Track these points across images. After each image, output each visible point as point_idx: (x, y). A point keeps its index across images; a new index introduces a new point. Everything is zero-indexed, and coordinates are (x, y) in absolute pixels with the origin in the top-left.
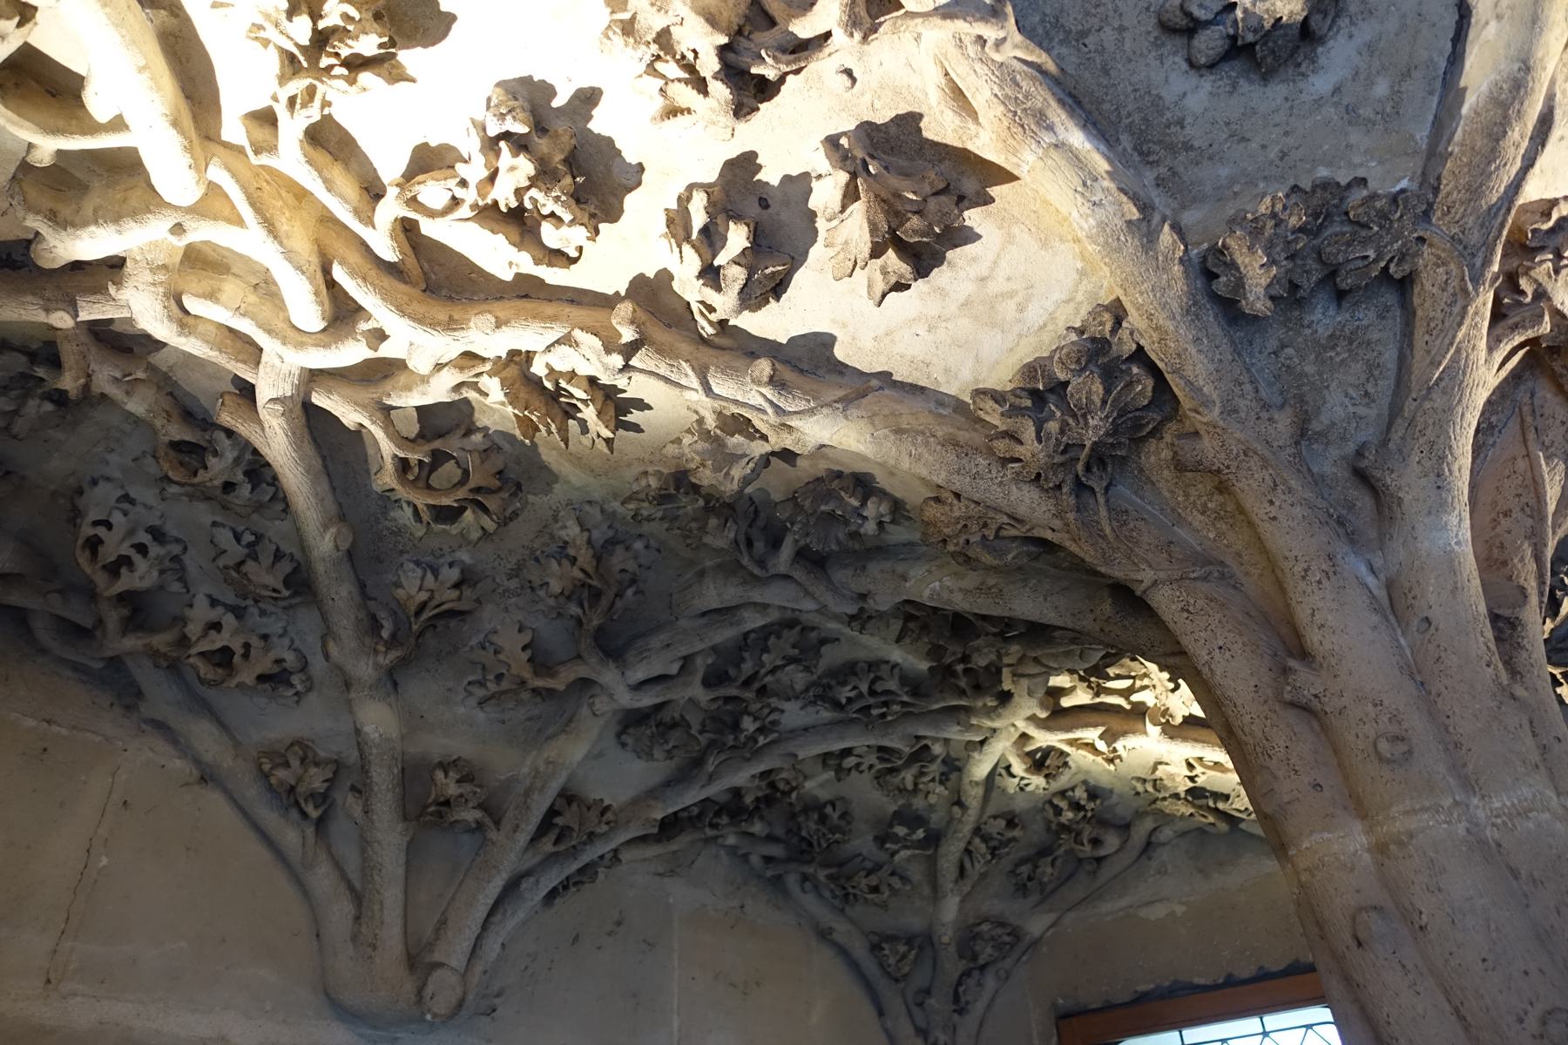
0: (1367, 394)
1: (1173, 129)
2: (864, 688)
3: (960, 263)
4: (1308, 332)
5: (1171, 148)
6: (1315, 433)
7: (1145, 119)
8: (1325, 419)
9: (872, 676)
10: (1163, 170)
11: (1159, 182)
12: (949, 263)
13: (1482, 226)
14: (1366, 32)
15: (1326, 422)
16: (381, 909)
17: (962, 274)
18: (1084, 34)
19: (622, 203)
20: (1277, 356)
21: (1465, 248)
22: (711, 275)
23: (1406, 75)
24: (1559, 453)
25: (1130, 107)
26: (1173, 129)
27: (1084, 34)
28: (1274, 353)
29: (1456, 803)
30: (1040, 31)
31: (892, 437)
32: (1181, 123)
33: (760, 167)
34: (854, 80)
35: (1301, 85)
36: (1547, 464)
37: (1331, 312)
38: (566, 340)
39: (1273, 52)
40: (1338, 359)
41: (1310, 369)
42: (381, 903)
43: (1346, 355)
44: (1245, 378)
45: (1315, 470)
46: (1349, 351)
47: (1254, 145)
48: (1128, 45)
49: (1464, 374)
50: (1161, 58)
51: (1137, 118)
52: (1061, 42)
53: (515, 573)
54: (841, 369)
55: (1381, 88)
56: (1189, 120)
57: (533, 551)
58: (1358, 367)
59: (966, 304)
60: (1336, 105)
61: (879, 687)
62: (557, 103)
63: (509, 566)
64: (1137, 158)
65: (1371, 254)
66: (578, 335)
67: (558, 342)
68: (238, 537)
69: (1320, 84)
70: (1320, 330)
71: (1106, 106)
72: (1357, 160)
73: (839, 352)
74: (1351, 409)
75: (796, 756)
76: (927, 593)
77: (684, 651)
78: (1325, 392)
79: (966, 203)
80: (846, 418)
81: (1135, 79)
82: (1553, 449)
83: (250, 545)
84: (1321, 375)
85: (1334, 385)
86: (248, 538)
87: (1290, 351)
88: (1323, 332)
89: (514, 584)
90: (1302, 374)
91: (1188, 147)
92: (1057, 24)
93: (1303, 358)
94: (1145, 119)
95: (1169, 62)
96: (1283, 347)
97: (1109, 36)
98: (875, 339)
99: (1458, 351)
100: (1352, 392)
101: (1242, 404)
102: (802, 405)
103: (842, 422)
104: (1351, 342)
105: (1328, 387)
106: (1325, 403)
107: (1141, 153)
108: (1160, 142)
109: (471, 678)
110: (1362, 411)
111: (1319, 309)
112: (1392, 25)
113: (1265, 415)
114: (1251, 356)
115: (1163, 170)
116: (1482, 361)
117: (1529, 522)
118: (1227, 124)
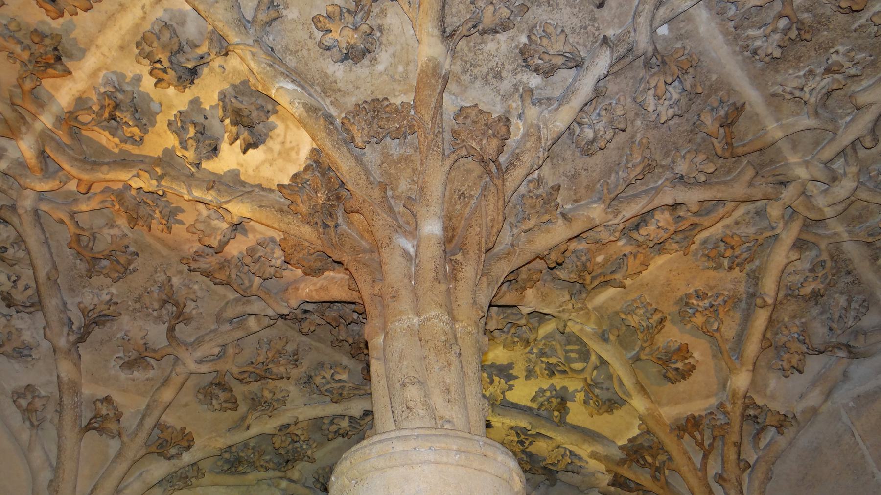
0: (413, 180)
1: (333, 84)
2: (328, 376)
3: (274, 137)
4: (391, 157)
5: (334, 91)
7: (323, 81)
8: (400, 190)
9: (333, 371)
10: (332, 99)
11: (332, 103)
12: (271, 138)
14: (391, 50)
16: (63, 473)
17: (276, 142)
18: (297, 52)
19: (155, 119)
22: (184, 145)
23: (408, 64)
25: (318, 76)
26: (333, 84)
27: (297, 52)
29: (409, 318)
30: (281, 51)
31: (258, 209)
32: (335, 82)
33: (201, 103)
34: (225, 69)
35: (373, 68)
38: (138, 176)
39: (356, 56)
42: (64, 470)
44: (362, 173)
45: (396, 210)
47: (362, 90)
48: (312, 54)
50: (324, 59)
51: (320, 80)
52: (290, 55)
53: (138, 300)
54: (243, 184)
55: (401, 69)
56: (338, 81)
57: (146, 289)
58: (409, 170)
59: (280, 153)
60: (387, 75)
61: (337, 377)
62: (127, 80)
63: (135, 296)
64: (322, 95)
65: (396, 125)
66: (141, 173)
67: (134, 176)
68: (9, 279)
69: (380, 68)
71: (309, 76)
72: (397, 94)
73: (243, 178)
74: (409, 186)
75: (298, 418)
76: (304, 294)
77: (220, 341)
79: (270, 114)
80: (242, 203)
81: (317, 67)
83: (14, 282)
84: (397, 173)
85: (402, 177)
86: (14, 278)
87: (385, 165)
89: (138, 306)
90: (391, 174)
91: (340, 91)
92: (287, 49)
93: (390, 168)
94: (323, 81)
95: (327, 61)
96: (383, 163)
97: (305, 52)
98: (253, 170)
100: (408, 180)
101: (360, 182)
102: (227, 199)
103: (241, 205)
104: (406, 160)
107: (324, 93)
108: (329, 89)
109: (118, 356)
110: (412, 187)
112: (399, 47)
113: (369, 186)
114: (372, 167)
115: (332, 99)
117: (479, 229)
118: (352, 82)
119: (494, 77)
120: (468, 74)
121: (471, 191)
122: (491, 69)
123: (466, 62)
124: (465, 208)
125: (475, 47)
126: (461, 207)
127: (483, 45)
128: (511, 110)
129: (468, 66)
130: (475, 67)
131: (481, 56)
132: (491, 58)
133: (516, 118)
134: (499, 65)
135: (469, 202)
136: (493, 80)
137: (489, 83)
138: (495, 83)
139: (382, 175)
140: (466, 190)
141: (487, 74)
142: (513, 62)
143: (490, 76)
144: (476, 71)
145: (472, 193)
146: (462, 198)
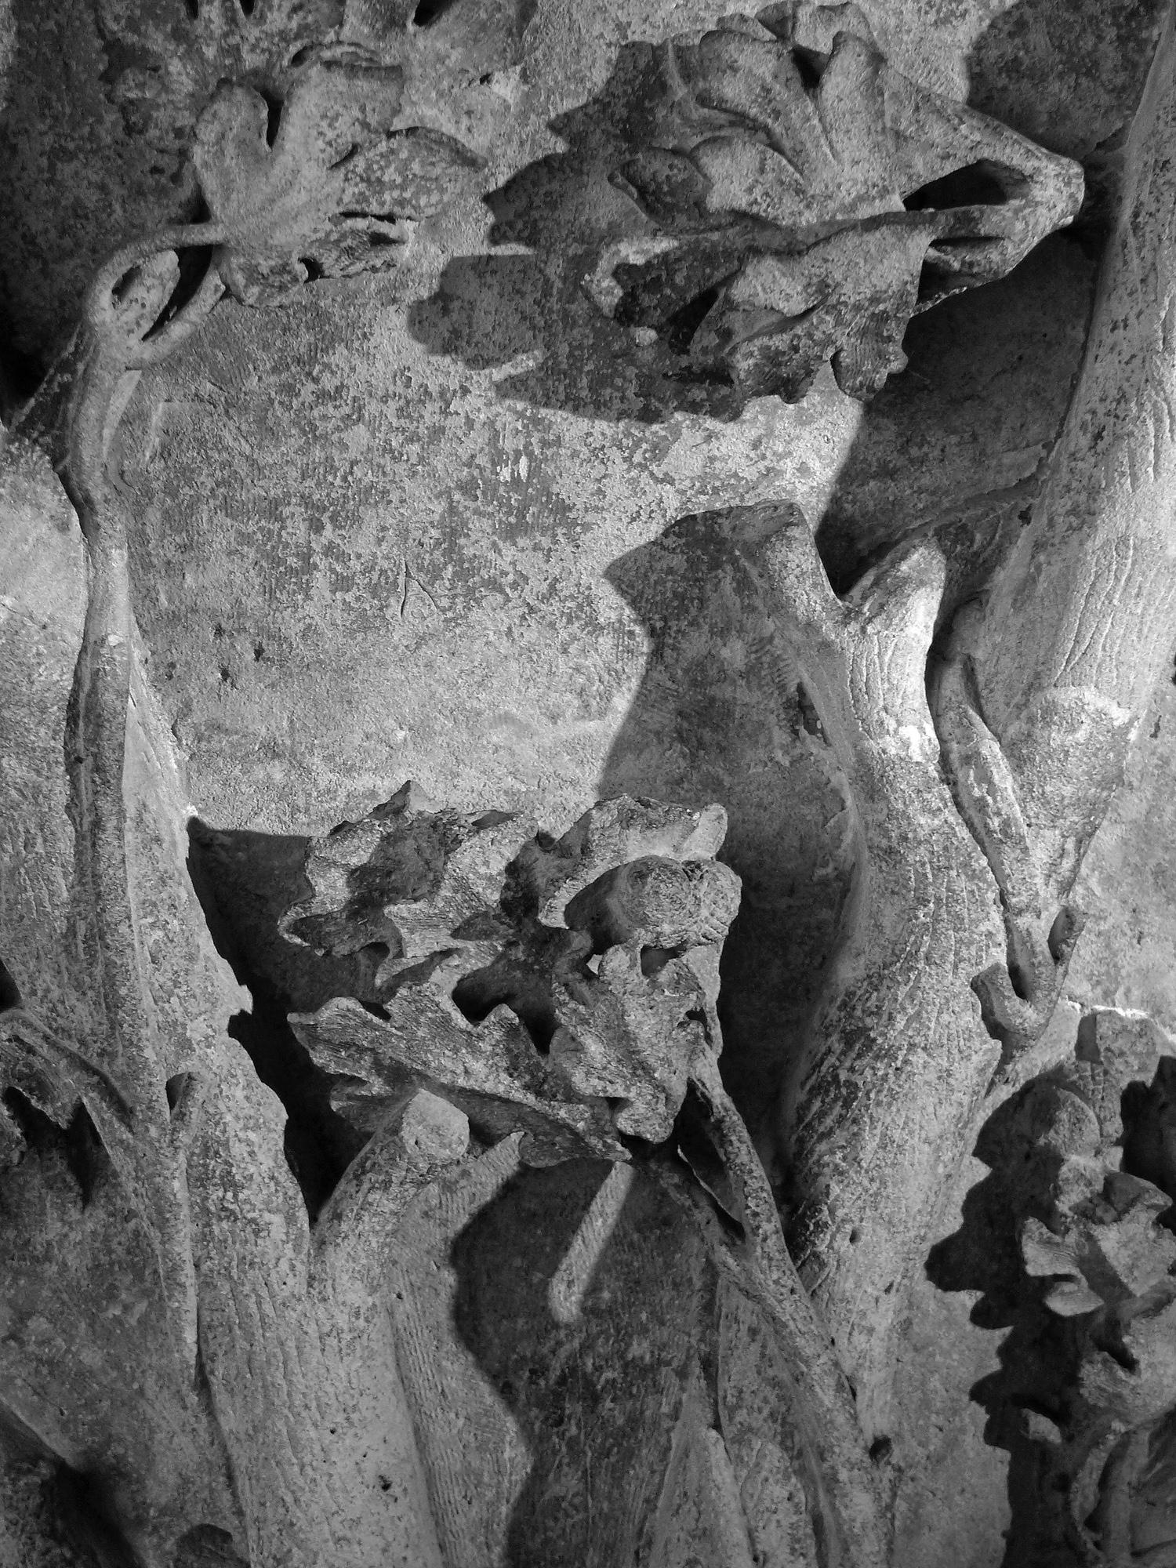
4: (51, 1269)
6: (163, 1512)
13: (78, 986)
15: (172, 1480)
20: (21, 1343)
21: (82, 1042)
24: (758, 1421)
28: (13, 1336)
36: (737, 1461)
37: (74, 1214)
40: (133, 1321)
41: (92, 1357)
43: (141, 1307)
46: (146, 1294)
49: (250, 1337)
70: (71, 1260)
78: (143, 1405)
82: (741, 1416)
84: (118, 1366)
85: (151, 1384)
87: (38, 1325)
88: (76, 1261)
90: (83, 1375)
96: (22, 1316)
99: (206, 1284)
105: (141, 1392)
106: (152, 1432)
111: (52, 1215)
116: (296, 1284)
119: (511, 533)
120: (320, 581)
121: (624, 1336)
122: (467, 488)
123: (273, 509)
124: (618, 1476)
125: (290, 390)
126: (588, 1477)
127: (339, 356)
128: (726, 692)
129: (297, 530)
130: (346, 518)
131: (359, 436)
132: (430, 413)
133: (780, 736)
134: (508, 444)
135: (634, 1421)
136: (509, 552)
137: (494, 585)
138: (529, 563)
139: (41, 1391)
140: (587, 1347)
141: (453, 532)
142: (599, 382)
143: (479, 537)
144: (362, 544)
145: (639, 1349)
146: (573, 1408)
